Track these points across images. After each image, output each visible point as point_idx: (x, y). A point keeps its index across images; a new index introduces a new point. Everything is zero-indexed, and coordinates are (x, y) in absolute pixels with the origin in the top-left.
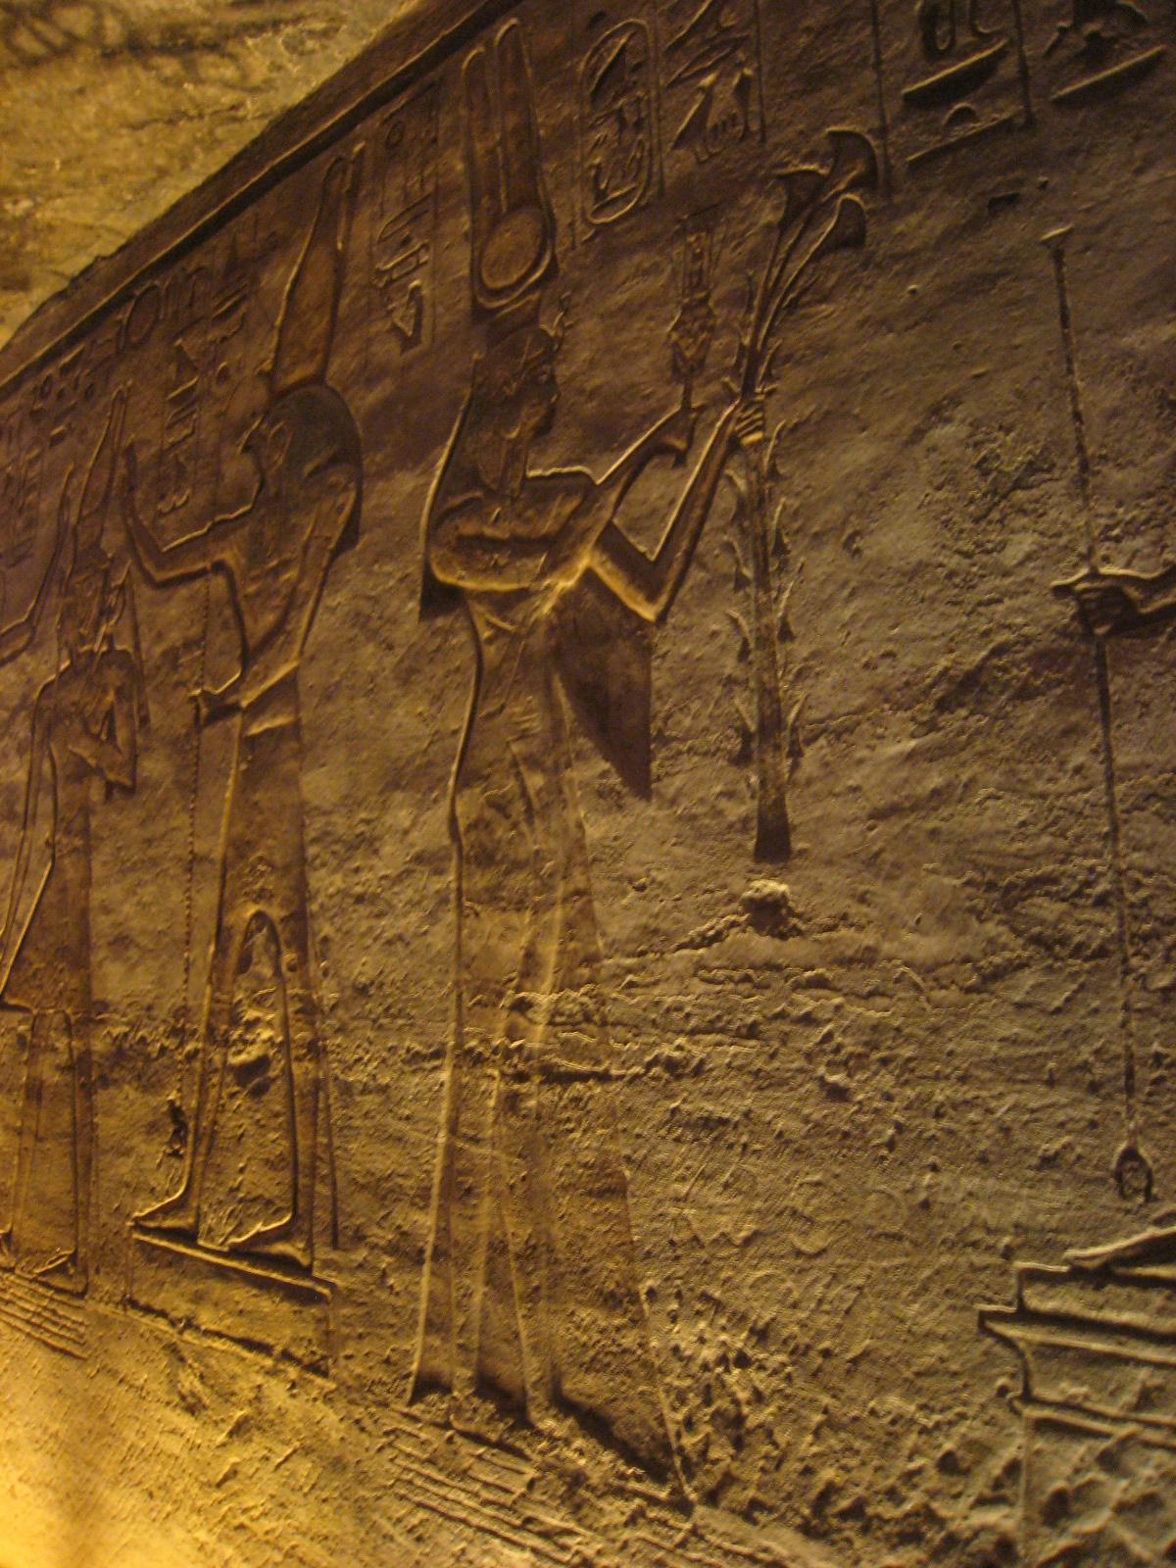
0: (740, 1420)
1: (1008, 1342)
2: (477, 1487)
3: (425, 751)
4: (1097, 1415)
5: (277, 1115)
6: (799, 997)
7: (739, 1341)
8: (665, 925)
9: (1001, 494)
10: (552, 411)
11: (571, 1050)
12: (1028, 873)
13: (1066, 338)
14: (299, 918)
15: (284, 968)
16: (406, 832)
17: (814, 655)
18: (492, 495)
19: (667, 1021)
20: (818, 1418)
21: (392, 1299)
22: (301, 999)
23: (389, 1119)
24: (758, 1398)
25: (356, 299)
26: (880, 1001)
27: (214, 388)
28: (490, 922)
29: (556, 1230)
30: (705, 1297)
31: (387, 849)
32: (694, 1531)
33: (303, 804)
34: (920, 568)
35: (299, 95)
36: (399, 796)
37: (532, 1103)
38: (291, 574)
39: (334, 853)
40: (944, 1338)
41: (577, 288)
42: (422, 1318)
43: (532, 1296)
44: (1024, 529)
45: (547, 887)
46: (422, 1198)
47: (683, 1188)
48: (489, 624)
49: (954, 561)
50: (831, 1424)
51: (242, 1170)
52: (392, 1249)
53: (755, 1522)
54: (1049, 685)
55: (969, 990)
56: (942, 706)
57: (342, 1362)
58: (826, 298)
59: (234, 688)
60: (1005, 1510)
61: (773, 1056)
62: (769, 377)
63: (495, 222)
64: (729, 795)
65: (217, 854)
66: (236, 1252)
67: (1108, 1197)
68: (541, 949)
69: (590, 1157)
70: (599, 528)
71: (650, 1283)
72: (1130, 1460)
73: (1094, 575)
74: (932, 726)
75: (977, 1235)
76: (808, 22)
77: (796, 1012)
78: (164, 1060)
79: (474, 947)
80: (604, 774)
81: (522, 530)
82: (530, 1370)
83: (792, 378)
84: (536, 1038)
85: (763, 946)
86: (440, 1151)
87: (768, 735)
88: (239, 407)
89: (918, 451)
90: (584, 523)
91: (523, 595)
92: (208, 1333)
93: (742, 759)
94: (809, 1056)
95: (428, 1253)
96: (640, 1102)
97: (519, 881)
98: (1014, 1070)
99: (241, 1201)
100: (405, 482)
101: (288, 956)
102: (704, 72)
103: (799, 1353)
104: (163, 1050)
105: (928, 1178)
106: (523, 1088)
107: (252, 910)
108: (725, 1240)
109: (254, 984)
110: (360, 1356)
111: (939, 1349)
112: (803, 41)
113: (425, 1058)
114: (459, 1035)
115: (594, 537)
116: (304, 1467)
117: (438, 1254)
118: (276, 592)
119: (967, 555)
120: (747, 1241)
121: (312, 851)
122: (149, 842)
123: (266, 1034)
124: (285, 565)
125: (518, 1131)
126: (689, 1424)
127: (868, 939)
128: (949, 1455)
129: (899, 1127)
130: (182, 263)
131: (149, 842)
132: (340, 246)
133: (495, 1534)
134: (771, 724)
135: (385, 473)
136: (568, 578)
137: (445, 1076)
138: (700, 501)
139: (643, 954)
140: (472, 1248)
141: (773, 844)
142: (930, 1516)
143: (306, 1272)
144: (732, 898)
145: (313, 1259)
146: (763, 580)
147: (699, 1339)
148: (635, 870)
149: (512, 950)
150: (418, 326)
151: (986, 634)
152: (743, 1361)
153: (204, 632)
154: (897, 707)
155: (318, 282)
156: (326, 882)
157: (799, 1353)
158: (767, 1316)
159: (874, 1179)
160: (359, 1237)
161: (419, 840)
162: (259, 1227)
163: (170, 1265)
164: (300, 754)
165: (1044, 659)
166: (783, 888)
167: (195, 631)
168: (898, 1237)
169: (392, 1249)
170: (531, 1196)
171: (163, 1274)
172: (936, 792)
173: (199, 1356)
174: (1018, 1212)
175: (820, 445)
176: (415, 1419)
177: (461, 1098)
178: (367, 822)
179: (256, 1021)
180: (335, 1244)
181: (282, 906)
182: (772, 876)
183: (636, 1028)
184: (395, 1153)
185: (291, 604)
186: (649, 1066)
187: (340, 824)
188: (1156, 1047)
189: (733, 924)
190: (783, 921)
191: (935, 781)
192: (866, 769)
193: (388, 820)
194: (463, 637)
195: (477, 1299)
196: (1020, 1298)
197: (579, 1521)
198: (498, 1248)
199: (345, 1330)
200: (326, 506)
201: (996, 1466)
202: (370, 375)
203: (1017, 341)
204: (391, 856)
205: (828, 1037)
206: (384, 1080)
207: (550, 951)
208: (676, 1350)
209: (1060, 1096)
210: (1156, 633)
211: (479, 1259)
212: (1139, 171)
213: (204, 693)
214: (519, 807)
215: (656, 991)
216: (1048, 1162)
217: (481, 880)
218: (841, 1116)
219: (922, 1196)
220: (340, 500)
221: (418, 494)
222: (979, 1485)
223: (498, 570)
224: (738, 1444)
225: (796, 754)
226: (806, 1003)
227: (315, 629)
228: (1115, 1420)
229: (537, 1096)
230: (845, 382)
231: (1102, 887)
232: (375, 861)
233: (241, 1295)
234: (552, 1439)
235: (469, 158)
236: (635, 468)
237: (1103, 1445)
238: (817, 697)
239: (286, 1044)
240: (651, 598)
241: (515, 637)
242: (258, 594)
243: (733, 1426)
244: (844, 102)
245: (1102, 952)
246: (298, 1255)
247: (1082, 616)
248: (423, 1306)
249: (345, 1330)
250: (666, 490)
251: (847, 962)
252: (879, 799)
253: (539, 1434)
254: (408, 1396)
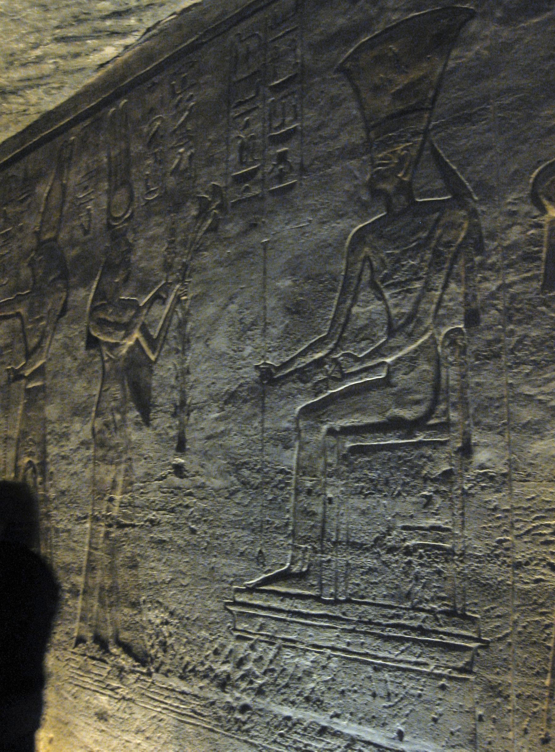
0: (166, 642)
1: (230, 612)
2: (92, 676)
4: (250, 633)
6: (185, 499)
7: (166, 616)
8: (152, 472)
9: (243, 331)
10: (129, 273)
11: (125, 516)
12: (242, 461)
13: (264, 279)
14: (43, 464)
16: (78, 432)
17: (195, 381)
18: (110, 303)
19: (149, 506)
20: (185, 640)
24: (171, 635)
25: (69, 208)
26: (205, 501)
28: (103, 468)
29: (120, 581)
30: (158, 602)
31: (72, 439)
32: (153, 683)
33: (45, 418)
34: (224, 353)
36: (77, 418)
37: (113, 535)
38: (43, 323)
40: (216, 611)
41: (139, 224)
42: (78, 616)
43: (111, 605)
44: (249, 345)
45: (119, 457)
46: (79, 572)
47: (153, 564)
48: (107, 355)
49: (232, 353)
50: (189, 642)
53: (167, 676)
54: (252, 399)
55: (226, 498)
56: (226, 403)
58: (206, 250)
59: (22, 368)
60: (228, 665)
61: (178, 518)
62: (190, 277)
63: (116, 188)
64: (170, 427)
65: (15, 436)
67: (254, 565)
68: (117, 479)
69: (129, 554)
70: (141, 323)
71: (144, 598)
72: (257, 646)
73: (265, 364)
74: (222, 409)
75: (225, 578)
76: (211, 137)
77: (185, 504)
79: (98, 477)
80: (137, 417)
81: (118, 319)
82: (108, 632)
83: (195, 278)
84: (115, 511)
85: (177, 481)
86: (86, 554)
87: (182, 408)
89: (225, 312)
90: (135, 321)
91: (117, 345)
93: (174, 415)
94: (187, 519)
95: (81, 592)
96: (142, 534)
97: (111, 454)
98: (235, 525)
100: (82, 292)
101: (39, 479)
102: (181, 146)
103: (181, 619)
105: (214, 560)
106: (111, 529)
107: (27, 460)
108: (163, 582)
111: (214, 615)
112: (208, 144)
114: (93, 510)
115: (138, 326)
117: (85, 592)
119: (235, 351)
120: (170, 582)
121: (48, 437)
124: (41, 319)
125: (109, 545)
126: (152, 646)
127: (203, 480)
128: (216, 649)
129: (208, 543)
133: (97, 692)
134: (183, 403)
135: (76, 287)
136: (130, 340)
137: (88, 525)
138: (168, 319)
139: (145, 482)
140: (94, 589)
141: (181, 447)
142: (211, 669)
144: (170, 464)
146: (184, 352)
147: (155, 616)
148: (145, 452)
149: (109, 479)
151: (238, 379)
152: (167, 623)
154: (215, 402)
156: (53, 450)
157: (181, 619)
158: (174, 607)
159: (201, 561)
164: (45, 398)
165: (252, 390)
166: (183, 461)
167: (9, 341)
168: (205, 579)
170: (112, 569)
172: (222, 432)
174: (234, 571)
175: (201, 305)
177: (93, 533)
178: (66, 427)
181: (38, 459)
182: (180, 457)
183: (142, 508)
184: (71, 554)
185: (43, 337)
186: (146, 521)
188: (267, 518)
189: (170, 473)
190: (181, 473)
191: (222, 428)
192: (205, 422)
194: (98, 359)
195: (95, 608)
196: (234, 597)
197: (122, 683)
198: (102, 589)
201: (226, 651)
202: (73, 243)
203: (253, 278)
205: (192, 512)
206: (69, 527)
207: (120, 479)
208: (150, 621)
209: (245, 533)
210: (276, 385)
211: (96, 593)
212: (287, 224)
214: (112, 426)
215: (149, 495)
216: (242, 554)
217: (100, 453)
218: (194, 539)
219: (212, 565)
221: (86, 298)
222: (222, 658)
223: (110, 334)
224: (165, 651)
225: (188, 415)
226: (188, 501)
228: (255, 634)
229: (115, 533)
230: (207, 282)
231: (258, 467)
234: (115, 656)
235: (109, 157)
236: (151, 302)
237: (251, 642)
238: (195, 396)
240: (153, 353)
241: (114, 361)
242: (32, 329)
243: (164, 645)
244: (217, 174)
245: (257, 488)
247: (262, 377)
248: (79, 611)
250: (160, 312)
251: (198, 487)
252: (209, 432)
253: (111, 654)
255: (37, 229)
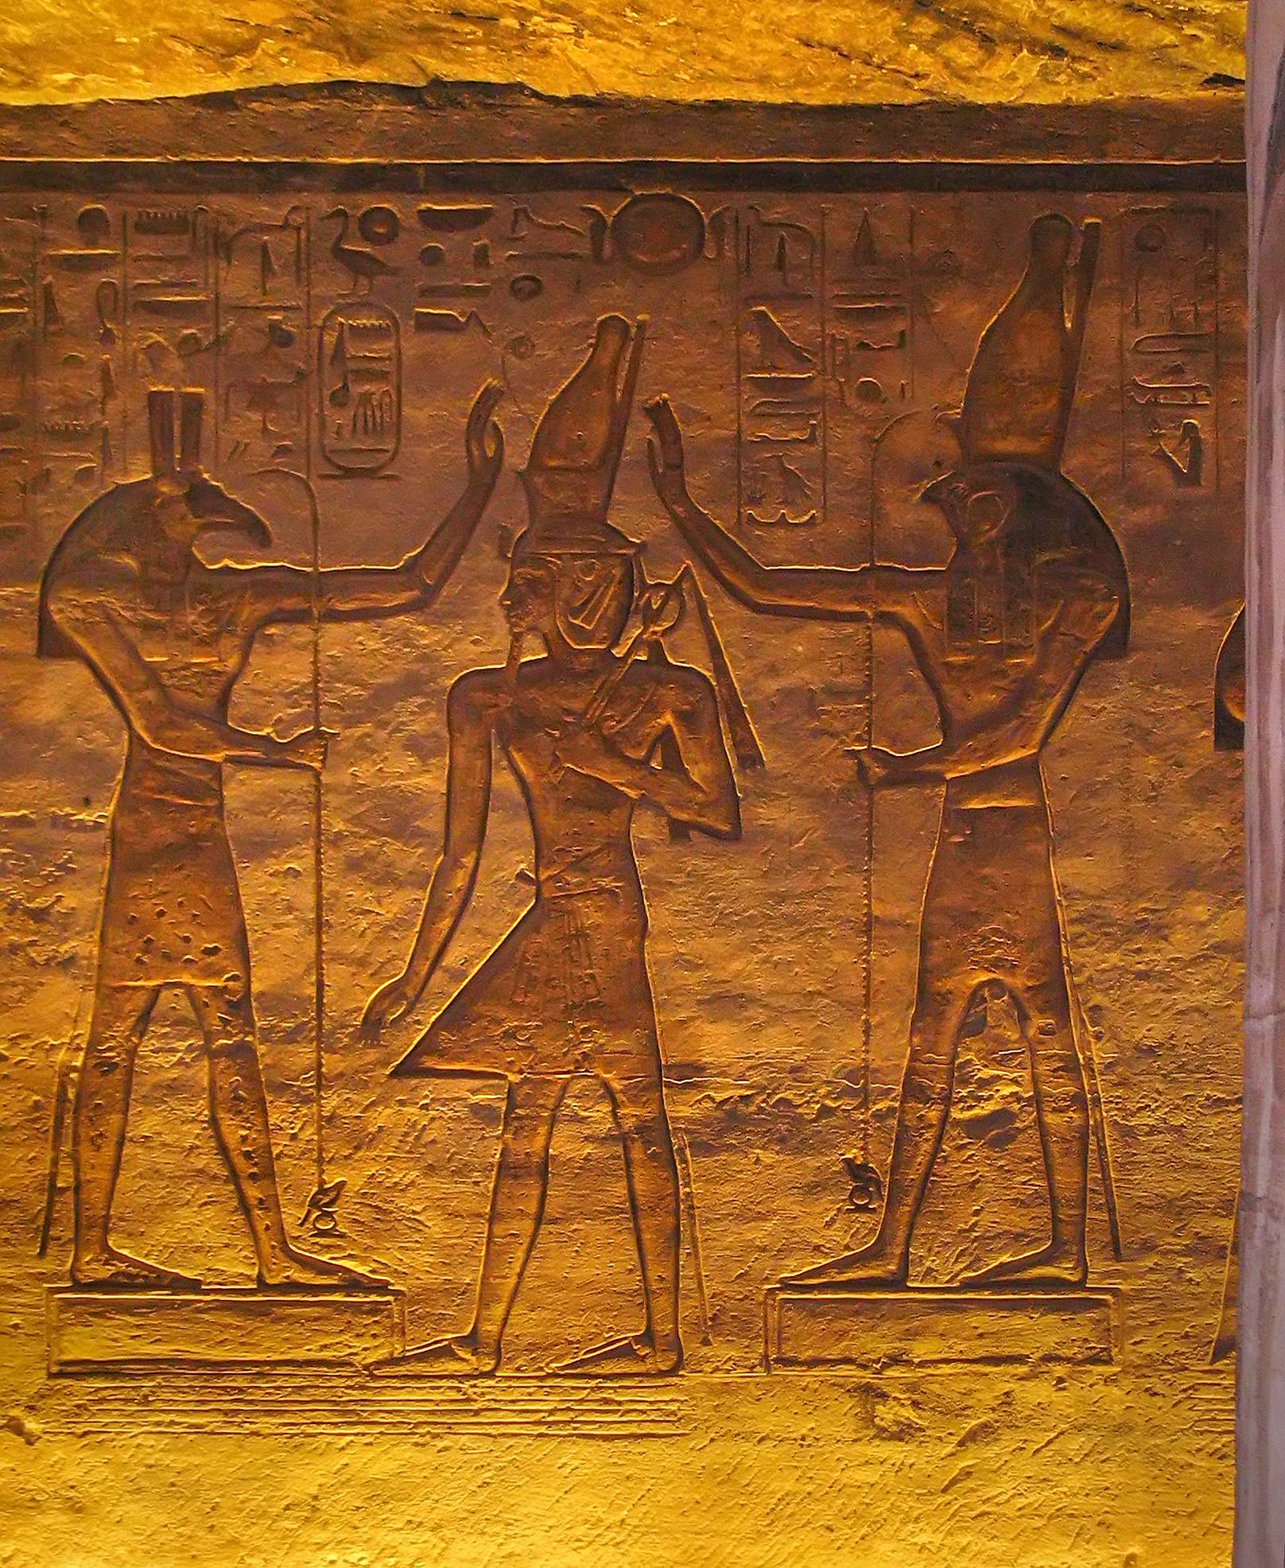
3: (1224, 861)
5: (1029, 1160)
15: (1031, 1032)
16: (1203, 925)
21: (1192, 1289)
22: (1061, 1058)
23: (1186, 1152)
27: (852, 401)
31: (1178, 936)
35: (990, 99)
38: (1029, 661)
39: (1107, 934)
51: (976, 1213)
52: (1188, 1251)
57: (1128, 1348)
66: (969, 1285)
78: (833, 1121)
88: (912, 442)
92: (922, 1364)
99: (976, 1239)
101: (1038, 1021)
104: (825, 1111)
107: (984, 977)
109: (991, 1045)
110: (1154, 1338)
113: (1228, 1103)
116: (1075, 1444)
118: (1003, 674)
122: (781, 898)
123: (1006, 1091)
124: (1014, 650)
130: (755, 198)
131: (781, 898)
132: (1069, 325)
143: (1080, 1285)
145: (1085, 1273)
150: (1195, 463)
153: (869, 686)
155: (1033, 355)
156: (1090, 960)
160: (1148, 1247)
161: (1219, 932)
162: (1005, 1258)
163: (857, 1313)
169: (1188, 1251)
171: (844, 1324)
173: (912, 1387)
176: (1220, 1372)
179: (997, 1078)
180: (1117, 1256)
181: (1029, 977)
185: (1023, 693)
187: (1115, 909)
193: (1180, 913)
199: (1131, 1323)
200: (1077, 607)
204: (1182, 943)
213: (870, 750)
220: (1099, 608)
227: (1067, 723)
232: (1163, 945)
233: (981, 1320)
239: (1037, 1101)
242: (966, 667)
246: (1066, 1275)
249: (1131, 1323)
254: (1210, 1357)
255: (955, 414)
